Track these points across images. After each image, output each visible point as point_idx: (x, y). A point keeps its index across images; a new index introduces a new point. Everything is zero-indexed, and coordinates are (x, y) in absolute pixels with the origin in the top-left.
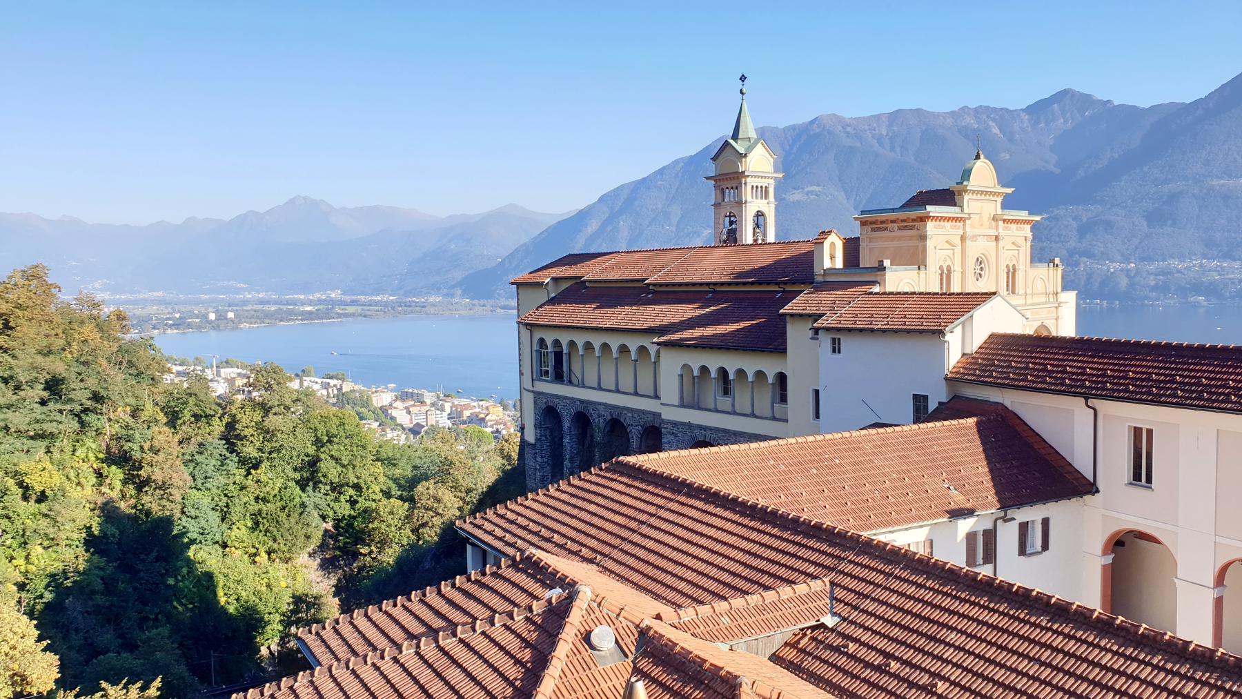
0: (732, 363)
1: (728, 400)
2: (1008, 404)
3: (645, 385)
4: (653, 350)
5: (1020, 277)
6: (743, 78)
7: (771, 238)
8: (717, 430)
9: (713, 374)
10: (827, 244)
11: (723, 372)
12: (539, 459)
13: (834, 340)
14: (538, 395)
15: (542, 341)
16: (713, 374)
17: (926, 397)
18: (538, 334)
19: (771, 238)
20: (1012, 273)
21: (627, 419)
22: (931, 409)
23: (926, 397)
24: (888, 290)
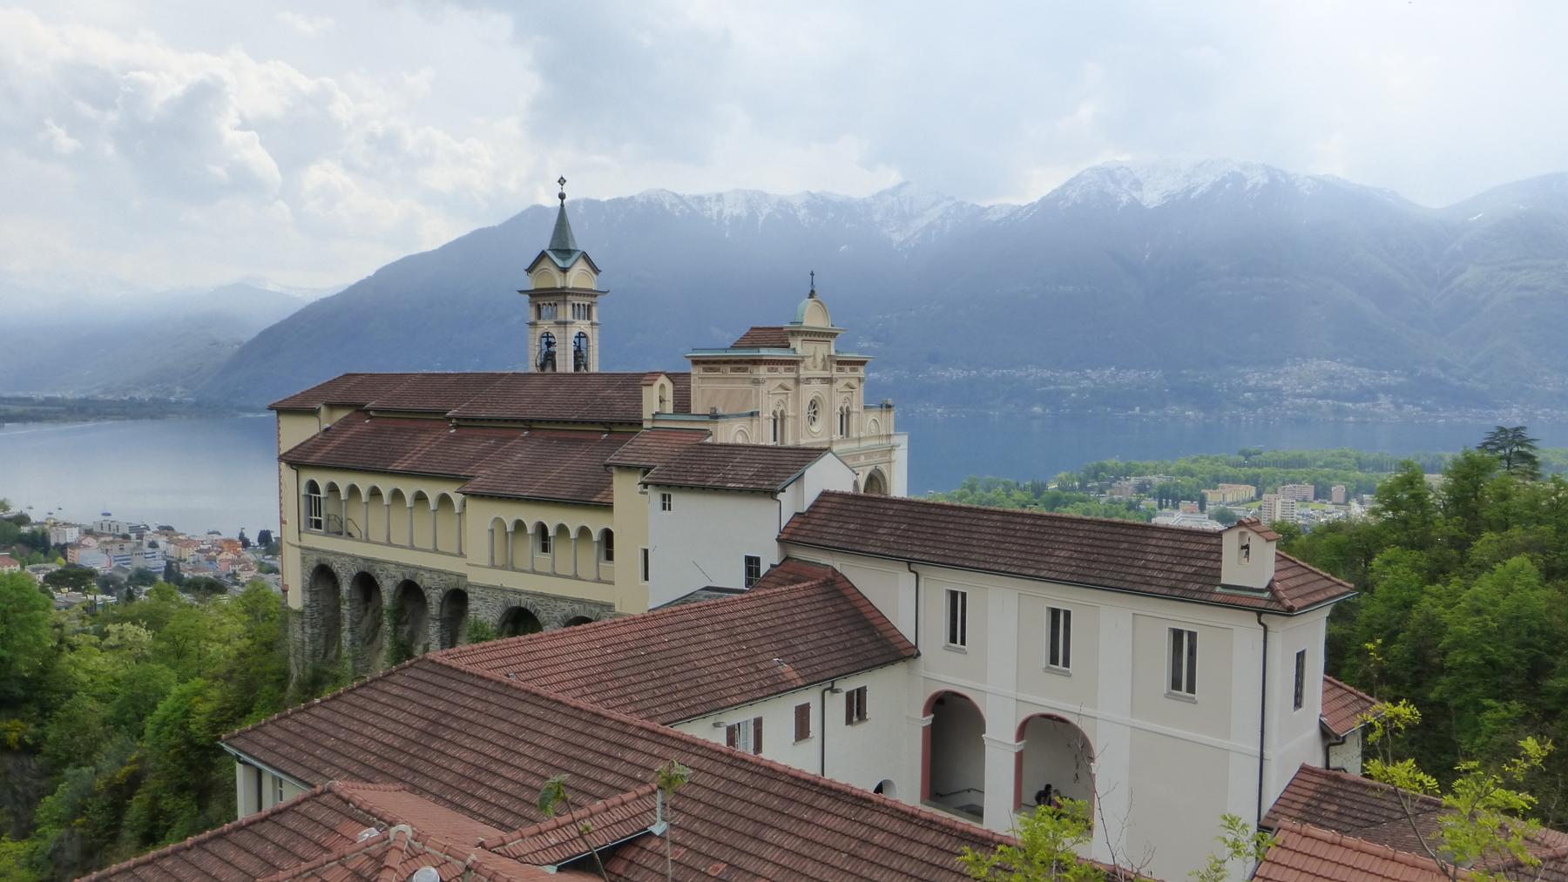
0: (553, 518)
1: (547, 557)
2: (837, 567)
3: (447, 541)
4: (457, 499)
5: (854, 419)
6: (562, 181)
7: (594, 367)
8: (535, 594)
9: (530, 530)
10: (657, 385)
11: (542, 529)
12: (309, 631)
13: (664, 497)
14: (306, 550)
15: (313, 487)
16: (530, 530)
17: (757, 560)
18: (307, 476)
19: (594, 367)
20: (845, 416)
21: (424, 581)
22: (762, 572)
23: (757, 560)
24: (719, 441)
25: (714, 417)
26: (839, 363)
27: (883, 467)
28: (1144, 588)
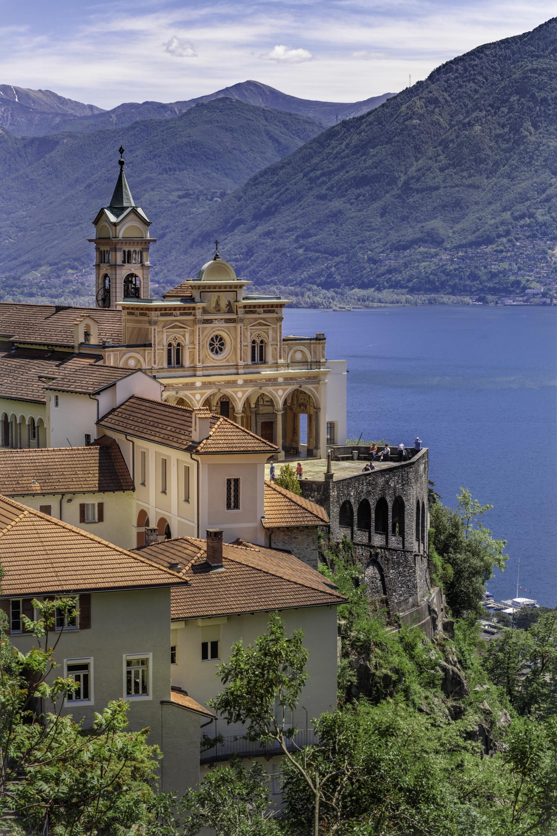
25: (104, 346)
26: (245, 307)
27: (309, 388)
28: (176, 445)
